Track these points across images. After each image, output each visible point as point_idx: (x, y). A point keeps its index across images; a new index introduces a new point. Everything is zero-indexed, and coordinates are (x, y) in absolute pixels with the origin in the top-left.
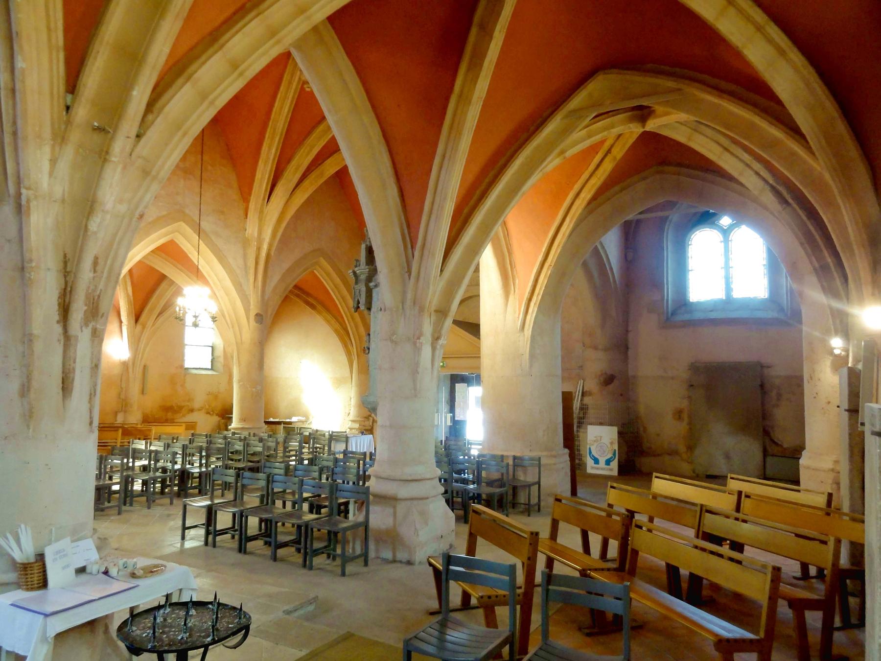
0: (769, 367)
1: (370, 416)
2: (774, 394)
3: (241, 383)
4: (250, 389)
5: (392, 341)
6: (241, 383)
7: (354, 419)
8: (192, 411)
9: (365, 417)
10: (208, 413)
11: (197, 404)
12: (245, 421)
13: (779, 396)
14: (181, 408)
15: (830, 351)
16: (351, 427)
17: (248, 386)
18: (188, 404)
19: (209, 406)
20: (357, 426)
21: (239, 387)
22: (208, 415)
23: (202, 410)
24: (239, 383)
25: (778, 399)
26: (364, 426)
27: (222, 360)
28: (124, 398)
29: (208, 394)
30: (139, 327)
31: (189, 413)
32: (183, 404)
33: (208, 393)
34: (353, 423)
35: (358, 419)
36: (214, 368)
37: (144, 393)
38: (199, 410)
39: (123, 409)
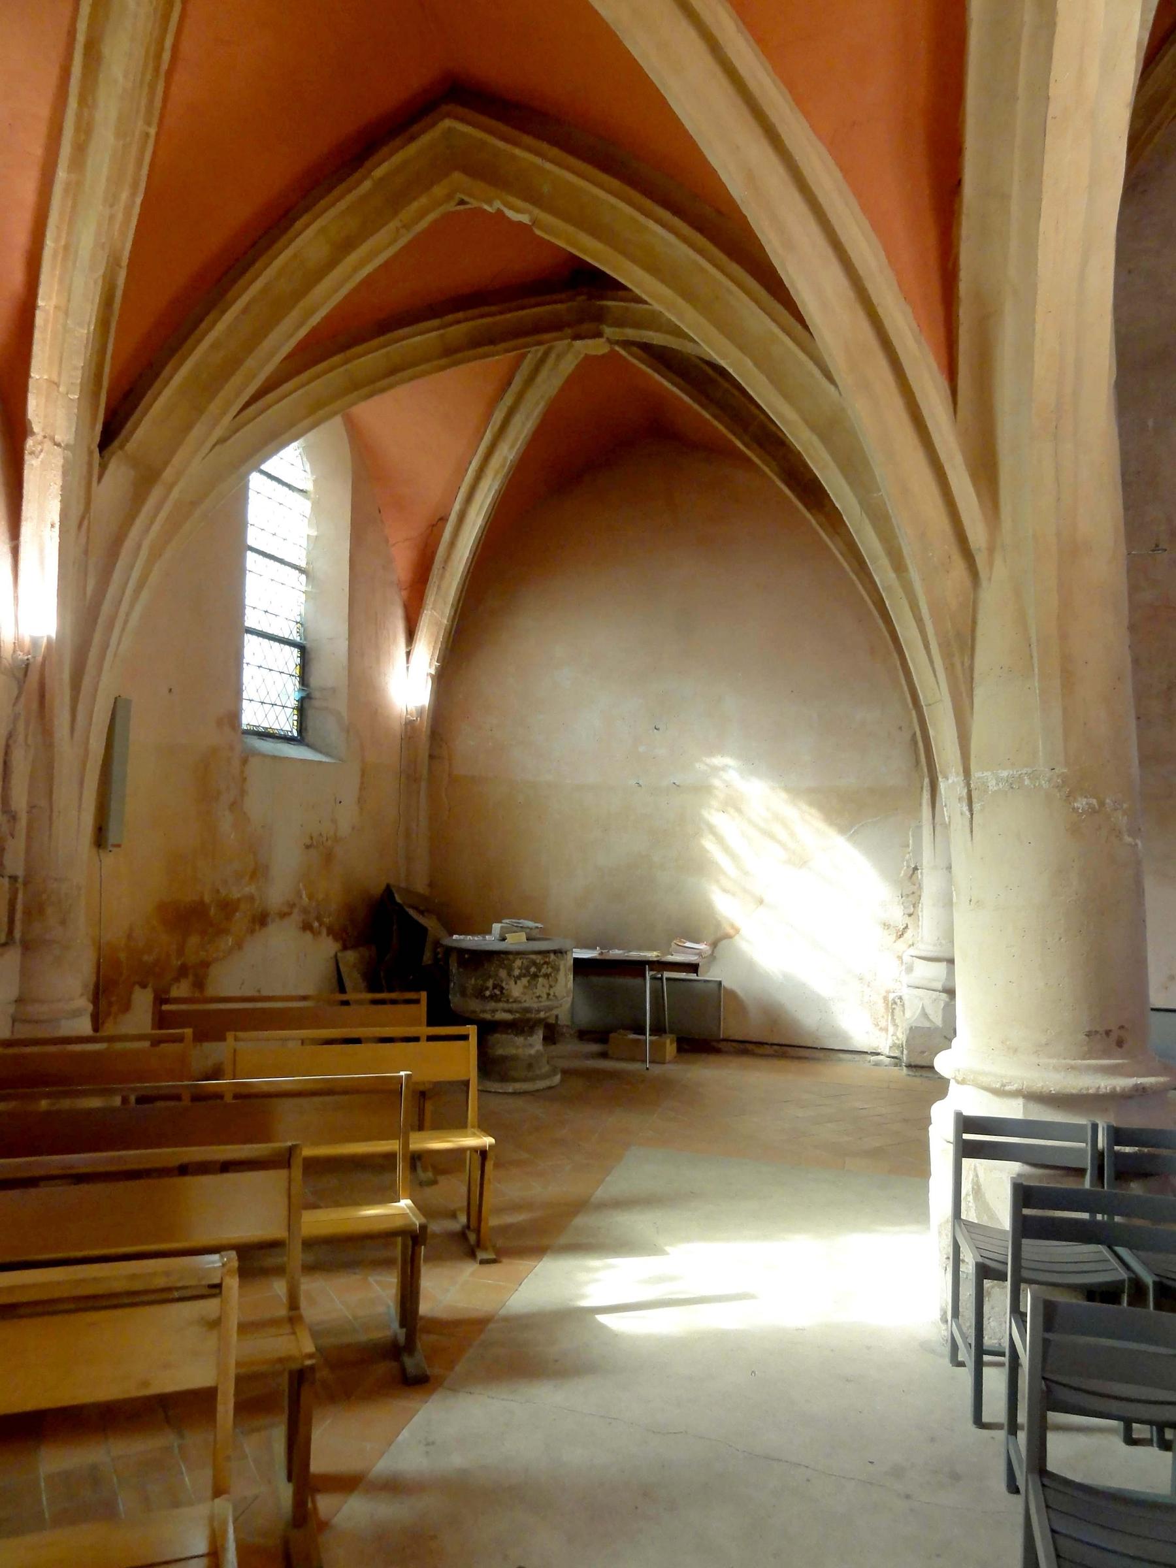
3: (1081, 803)
4: (1128, 839)
6: (1081, 803)
8: (261, 919)
10: (306, 927)
11: (277, 892)
12: (1120, 1043)
14: (228, 907)
17: (1121, 820)
18: (251, 889)
19: (311, 897)
21: (1075, 830)
22: (308, 936)
23: (289, 914)
24: (1070, 797)
27: (341, 704)
28: (20, 872)
29: (308, 847)
30: (119, 474)
31: (252, 931)
32: (236, 894)
33: (308, 842)
36: (310, 736)
37: (112, 837)
38: (283, 915)
39: (17, 935)
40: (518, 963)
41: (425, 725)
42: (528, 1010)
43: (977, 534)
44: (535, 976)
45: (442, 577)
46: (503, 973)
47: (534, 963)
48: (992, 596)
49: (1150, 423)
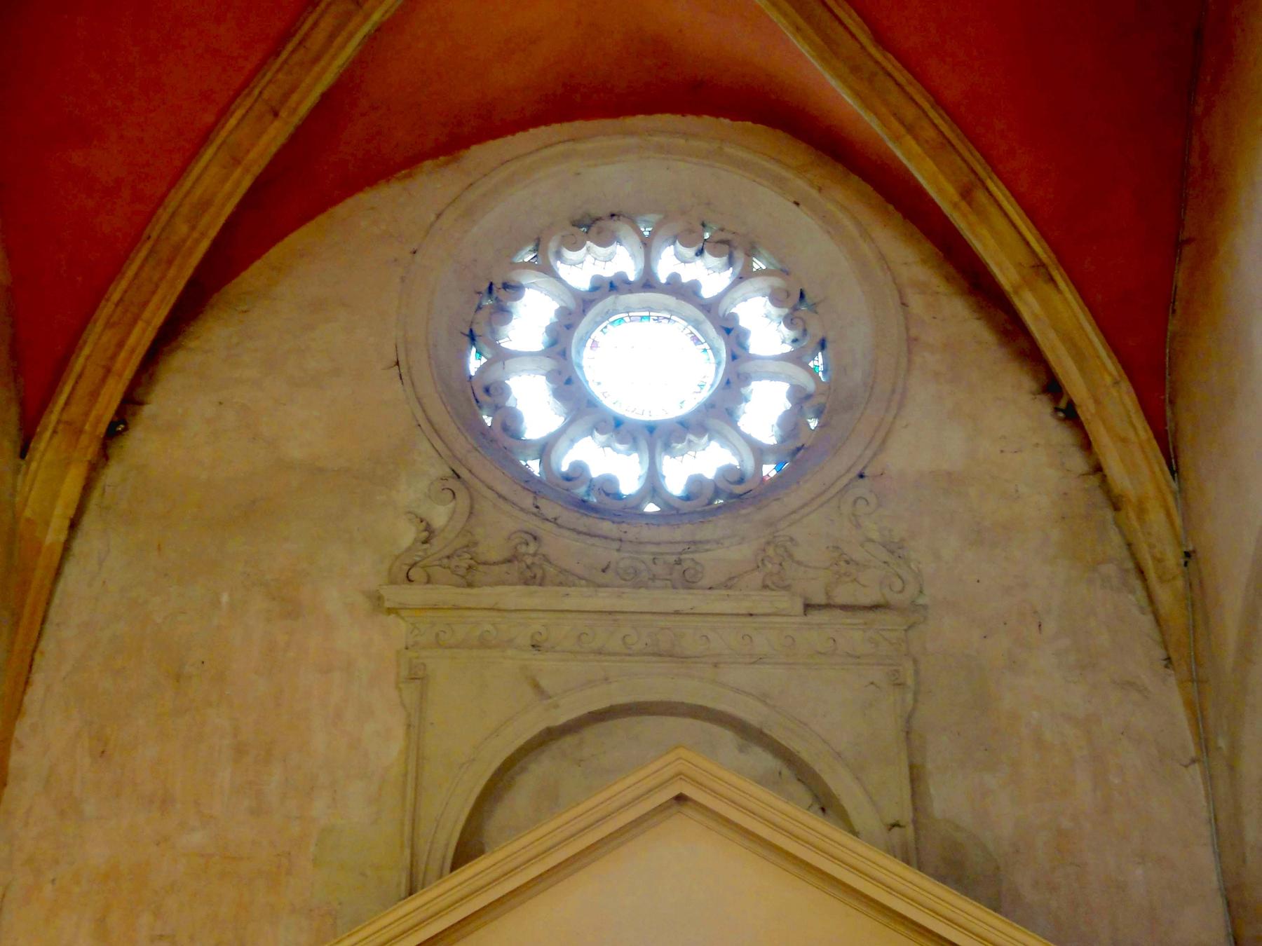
49: (225, 598)
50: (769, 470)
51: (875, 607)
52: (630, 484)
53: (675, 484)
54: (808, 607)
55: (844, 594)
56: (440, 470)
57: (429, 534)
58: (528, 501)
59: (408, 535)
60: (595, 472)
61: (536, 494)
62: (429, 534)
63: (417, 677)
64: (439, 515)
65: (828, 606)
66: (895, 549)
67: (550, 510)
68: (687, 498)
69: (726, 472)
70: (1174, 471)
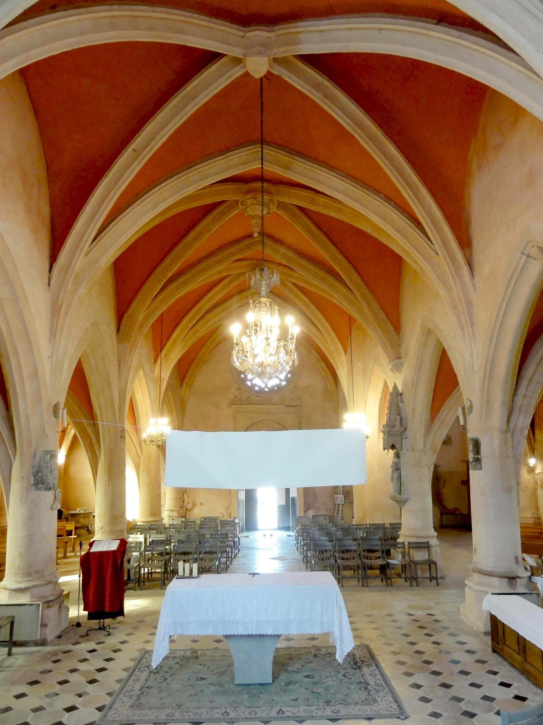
0: (439, 467)
1: (183, 506)
2: (442, 481)
3: (150, 487)
5: (420, 467)
6: (150, 487)
7: (174, 509)
9: (181, 507)
13: (444, 482)
15: (527, 465)
16: (171, 515)
20: (175, 514)
24: (149, 486)
25: (444, 484)
26: (180, 513)
34: (172, 512)
35: (175, 509)
40: (82, 515)
41: (63, 467)
42: (83, 524)
43: (140, 454)
44: (85, 518)
45: (68, 435)
46: (79, 517)
47: (85, 515)
48: (142, 462)
50: (284, 383)
51: (296, 406)
52: (263, 386)
53: (269, 386)
54: (287, 406)
55: (292, 404)
56: (236, 387)
57: (235, 396)
58: (249, 391)
59: (233, 397)
60: (258, 384)
61: (250, 390)
62: (235, 396)
63: (235, 417)
64: (237, 394)
65: (289, 406)
66: (299, 398)
67: (252, 393)
68: (271, 388)
69: (276, 384)
70: (337, 387)
